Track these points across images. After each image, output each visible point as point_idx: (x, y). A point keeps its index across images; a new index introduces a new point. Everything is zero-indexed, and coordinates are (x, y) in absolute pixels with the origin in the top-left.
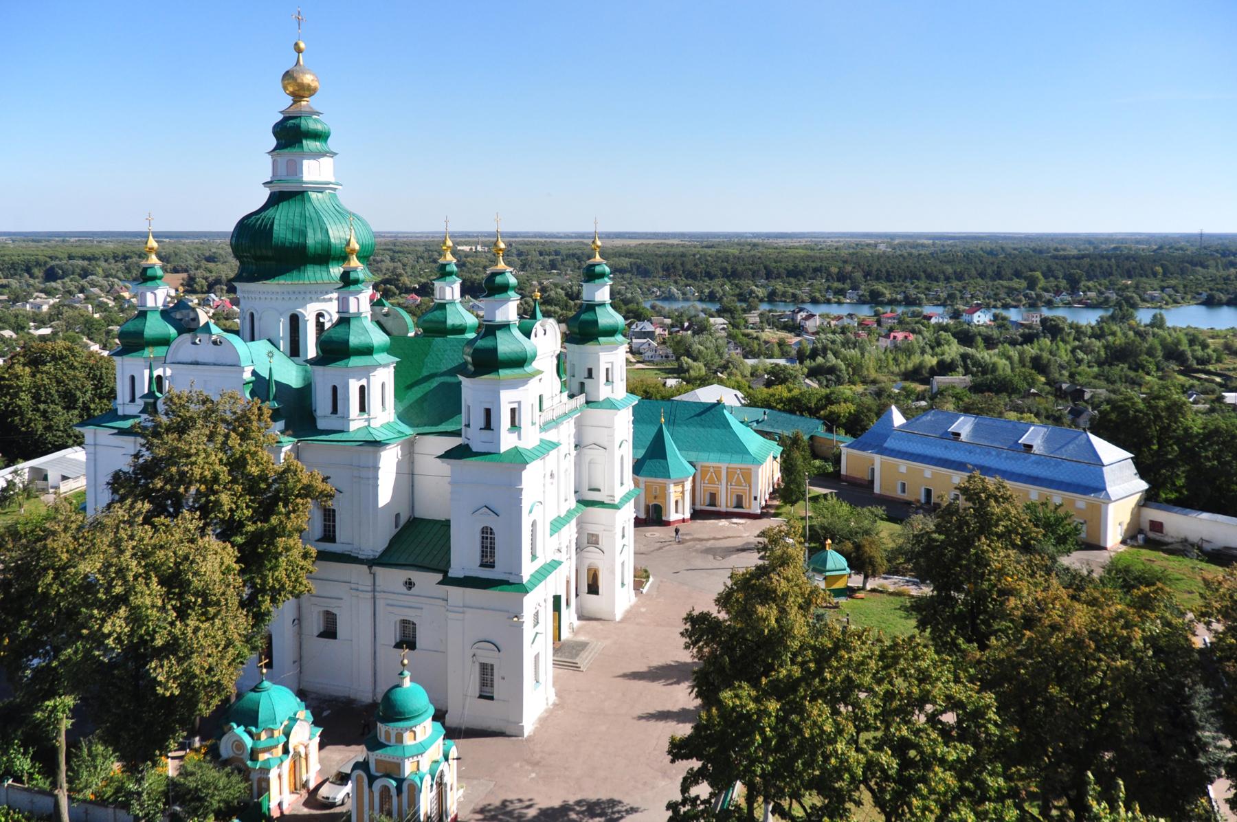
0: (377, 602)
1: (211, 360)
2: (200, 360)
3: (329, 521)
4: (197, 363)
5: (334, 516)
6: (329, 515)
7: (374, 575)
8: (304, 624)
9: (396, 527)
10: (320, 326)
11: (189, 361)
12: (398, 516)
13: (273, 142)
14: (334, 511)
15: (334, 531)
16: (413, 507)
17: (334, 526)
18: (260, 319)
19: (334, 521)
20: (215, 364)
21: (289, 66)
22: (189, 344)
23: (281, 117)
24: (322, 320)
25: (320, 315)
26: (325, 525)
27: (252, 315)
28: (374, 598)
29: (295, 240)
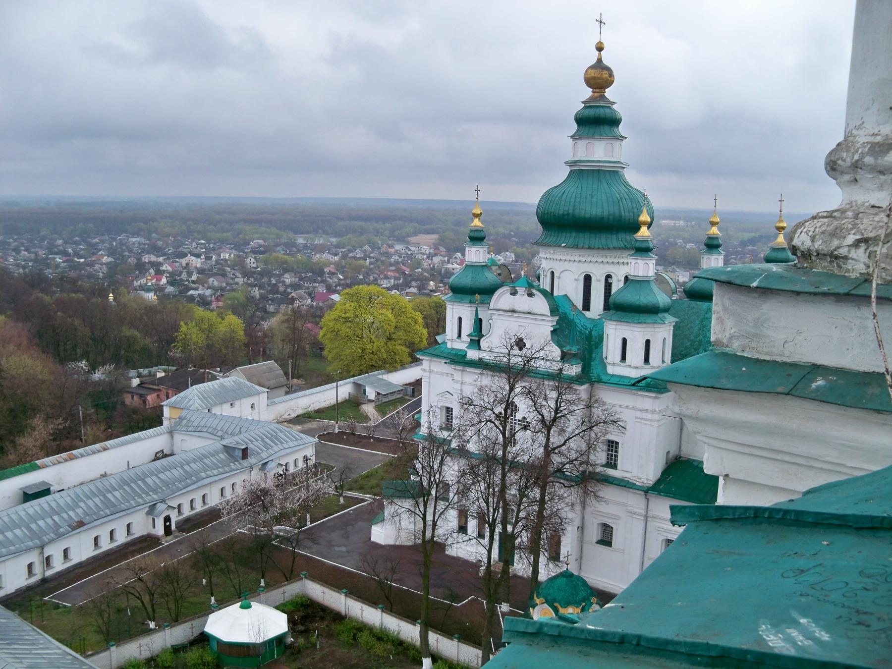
0: (648, 523)
1: (525, 308)
2: (517, 308)
3: (612, 451)
4: (514, 311)
5: (617, 447)
6: (612, 447)
7: (648, 499)
8: (586, 532)
9: (667, 463)
10: (608, 286)
11: (508, 308)
12: (668, 453)
13: (575, 127)
14: (617, 443)
15: (615, 460)
16: (680, 447)
17: (616, 456)
18: (559, 278)
19: (617, 452)
20: (529, 313)
21: (594, 61)
22: (508, 294)
23: (583, 105)
24: (610, 281)
25: (608, 277)
26: (608, 454)
27: (553, 273)
28: (646, 517)
29: (594, 213)
